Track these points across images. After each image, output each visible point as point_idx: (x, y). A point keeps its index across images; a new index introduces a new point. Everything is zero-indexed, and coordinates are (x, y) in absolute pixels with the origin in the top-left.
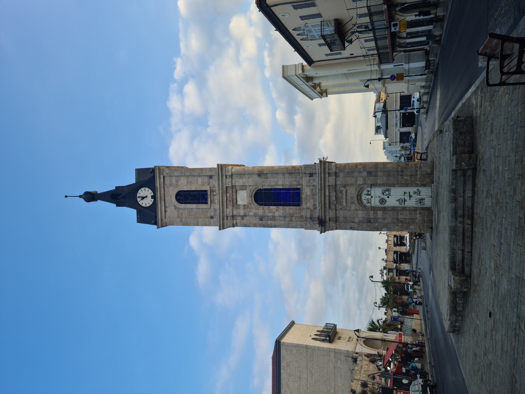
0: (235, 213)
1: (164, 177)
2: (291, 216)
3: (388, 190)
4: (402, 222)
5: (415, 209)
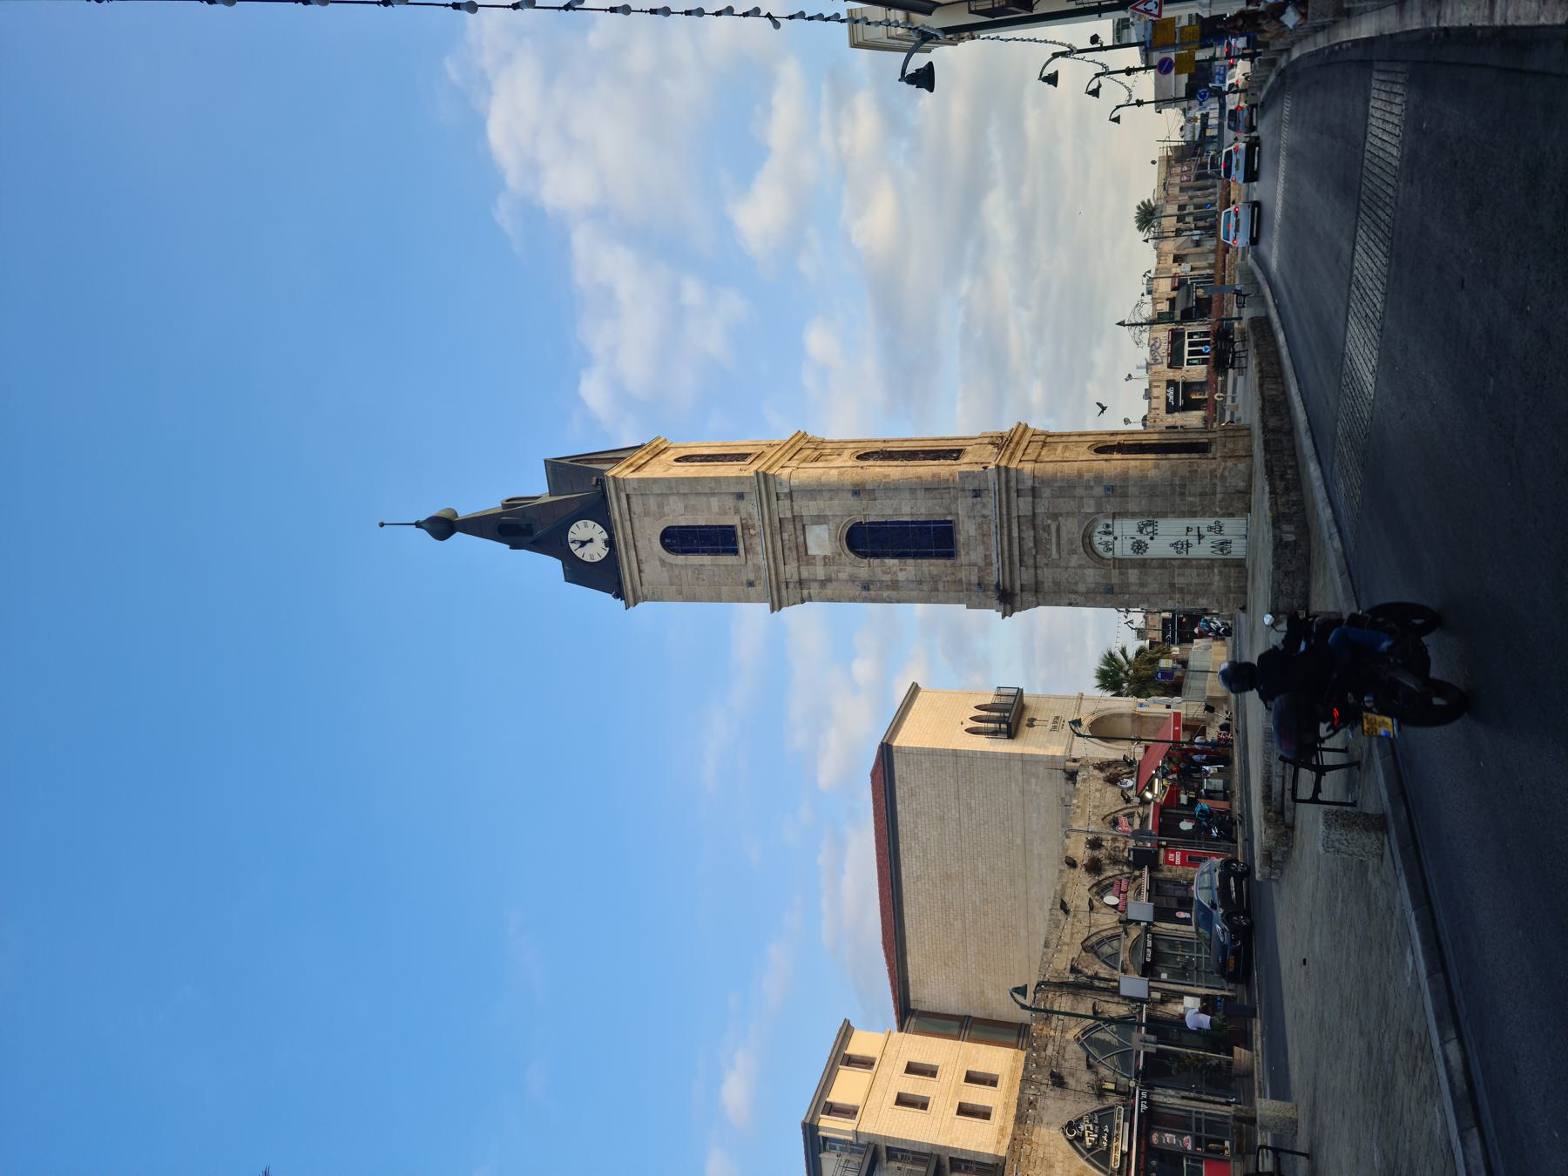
0: (805, 574)
1: (628, 496)
2: (935, 580)
3: (1152, 524)
4: (1181, 590)
5: (1211, 563)
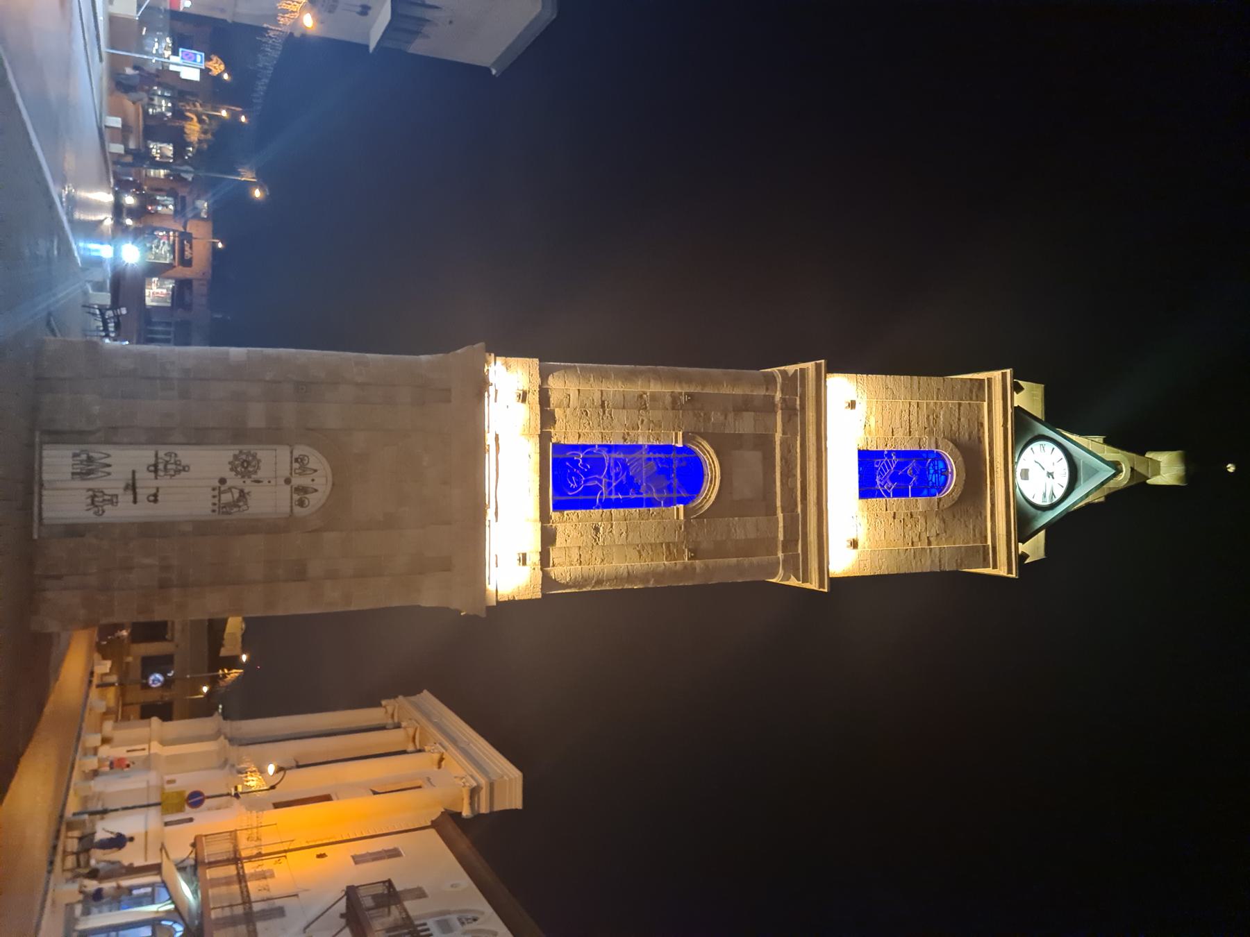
3: (225, 508)
5: (113, 434)
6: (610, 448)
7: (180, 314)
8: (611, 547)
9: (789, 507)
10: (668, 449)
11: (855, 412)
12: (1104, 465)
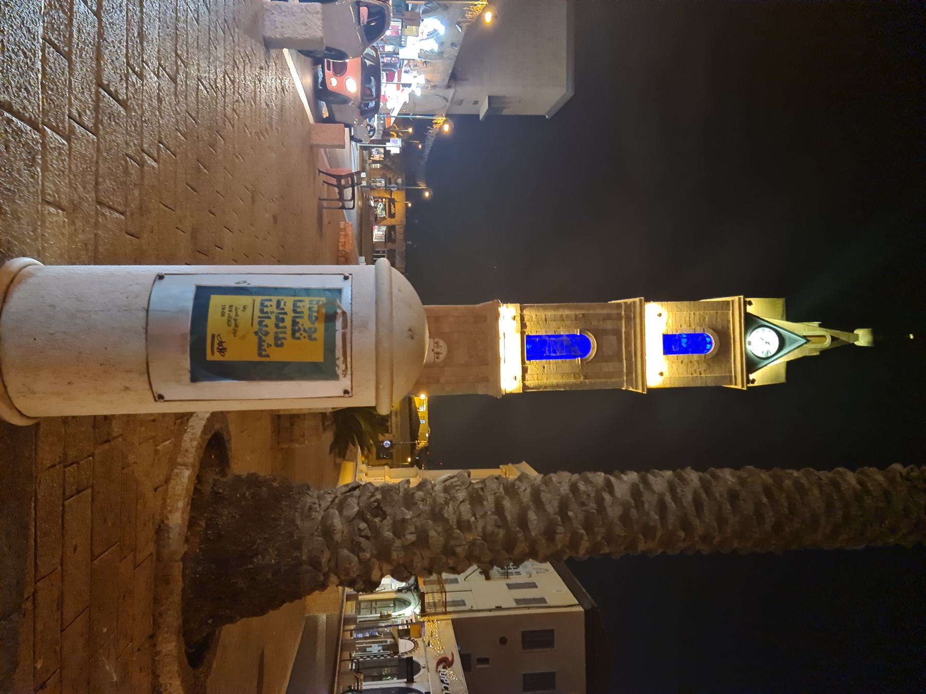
6: (549, 336)
7: (389, 245)
8: (548, 374)
9: (629, 359)
10: (574, 336)
11: (659, 318)
12: (811, 337)
